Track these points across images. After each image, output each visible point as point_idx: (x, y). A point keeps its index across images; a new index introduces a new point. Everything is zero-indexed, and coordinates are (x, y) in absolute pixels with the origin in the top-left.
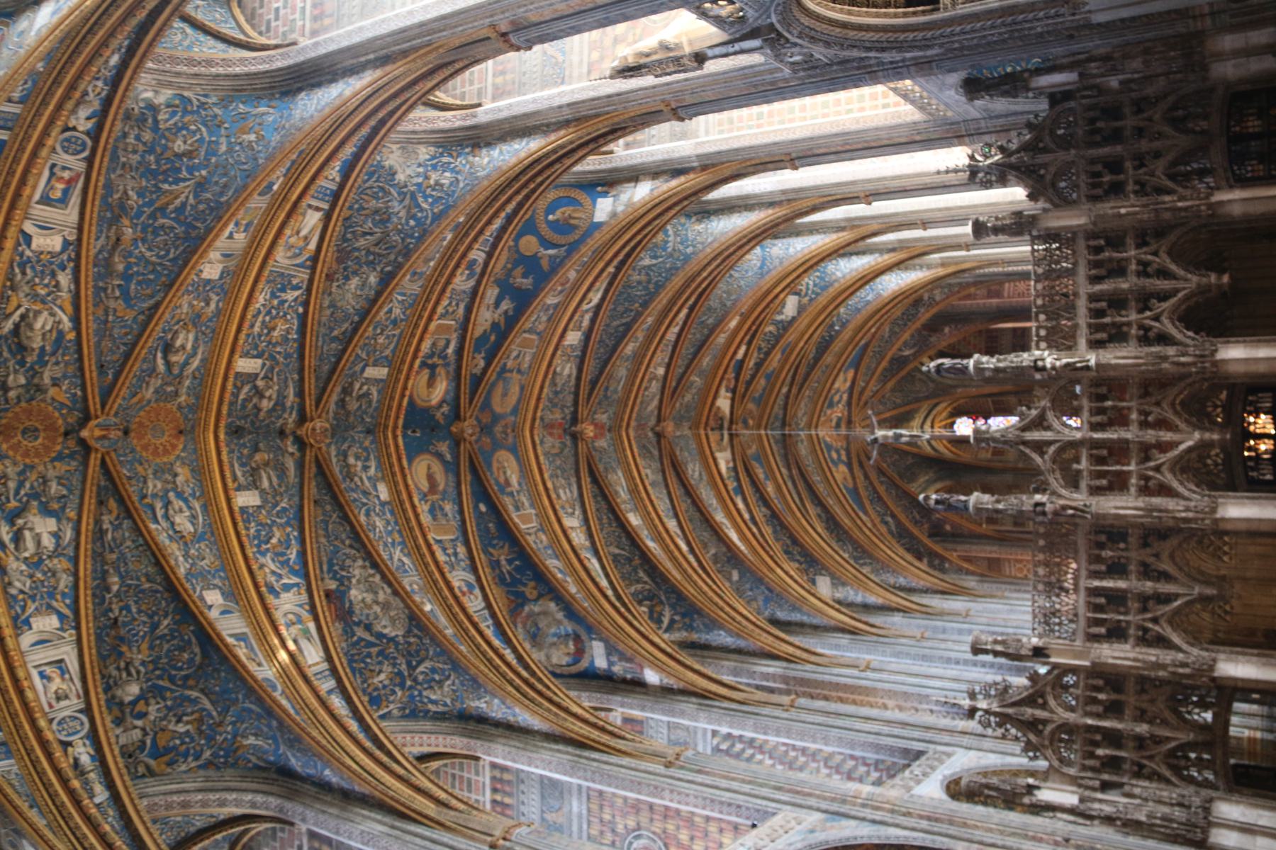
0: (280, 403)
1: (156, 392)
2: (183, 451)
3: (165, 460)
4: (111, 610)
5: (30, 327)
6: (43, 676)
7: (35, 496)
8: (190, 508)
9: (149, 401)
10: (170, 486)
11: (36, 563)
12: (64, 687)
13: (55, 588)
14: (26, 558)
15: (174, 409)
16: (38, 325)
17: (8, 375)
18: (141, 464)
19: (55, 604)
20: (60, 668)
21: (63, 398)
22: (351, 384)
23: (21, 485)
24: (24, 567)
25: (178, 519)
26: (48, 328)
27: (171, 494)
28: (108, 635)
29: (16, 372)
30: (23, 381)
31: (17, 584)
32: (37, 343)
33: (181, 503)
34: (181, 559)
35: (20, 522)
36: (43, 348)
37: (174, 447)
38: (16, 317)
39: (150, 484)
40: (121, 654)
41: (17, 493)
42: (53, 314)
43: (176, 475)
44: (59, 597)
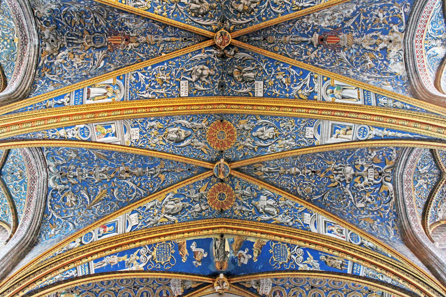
0: (204, 62)
1: (200, 140)
2: (231, 122)
3: (236, 133)
4: (308, 173)
5: (174, 208)
6: (331, 232)
7: (250, 201)
8: (261, 126)
9: (206, 143)
10: (249, 134)
11: (280, 211)
12: (337, 228)
13: (293, 207)
14: (277, 213)
15: (209, 128)
16: (172, 207)
17: (195, 212)
18: (237, 147)
19: (299, 211)
20: (329, 225)
21: (205, 186)
22: (192, 11)
23: (244, 205)
24: (281, 215)
25: (267, 135)
26: (173, 202)
27: (254, 134)
28: (319, 177)
29: (194, 209)
30: (198, 205)
31: (288, 221)
32: (180, 204)
33: (258, 130)
34: (287, 141)
35: (261, 210)
36: (182, 201)
37: (229, 127)
38: (169, 217)
39: (248, 144)
40: (330, 172)
41: (248, 207)
42: (167, 202)
43: (244, 128)
44: (297, 208)
